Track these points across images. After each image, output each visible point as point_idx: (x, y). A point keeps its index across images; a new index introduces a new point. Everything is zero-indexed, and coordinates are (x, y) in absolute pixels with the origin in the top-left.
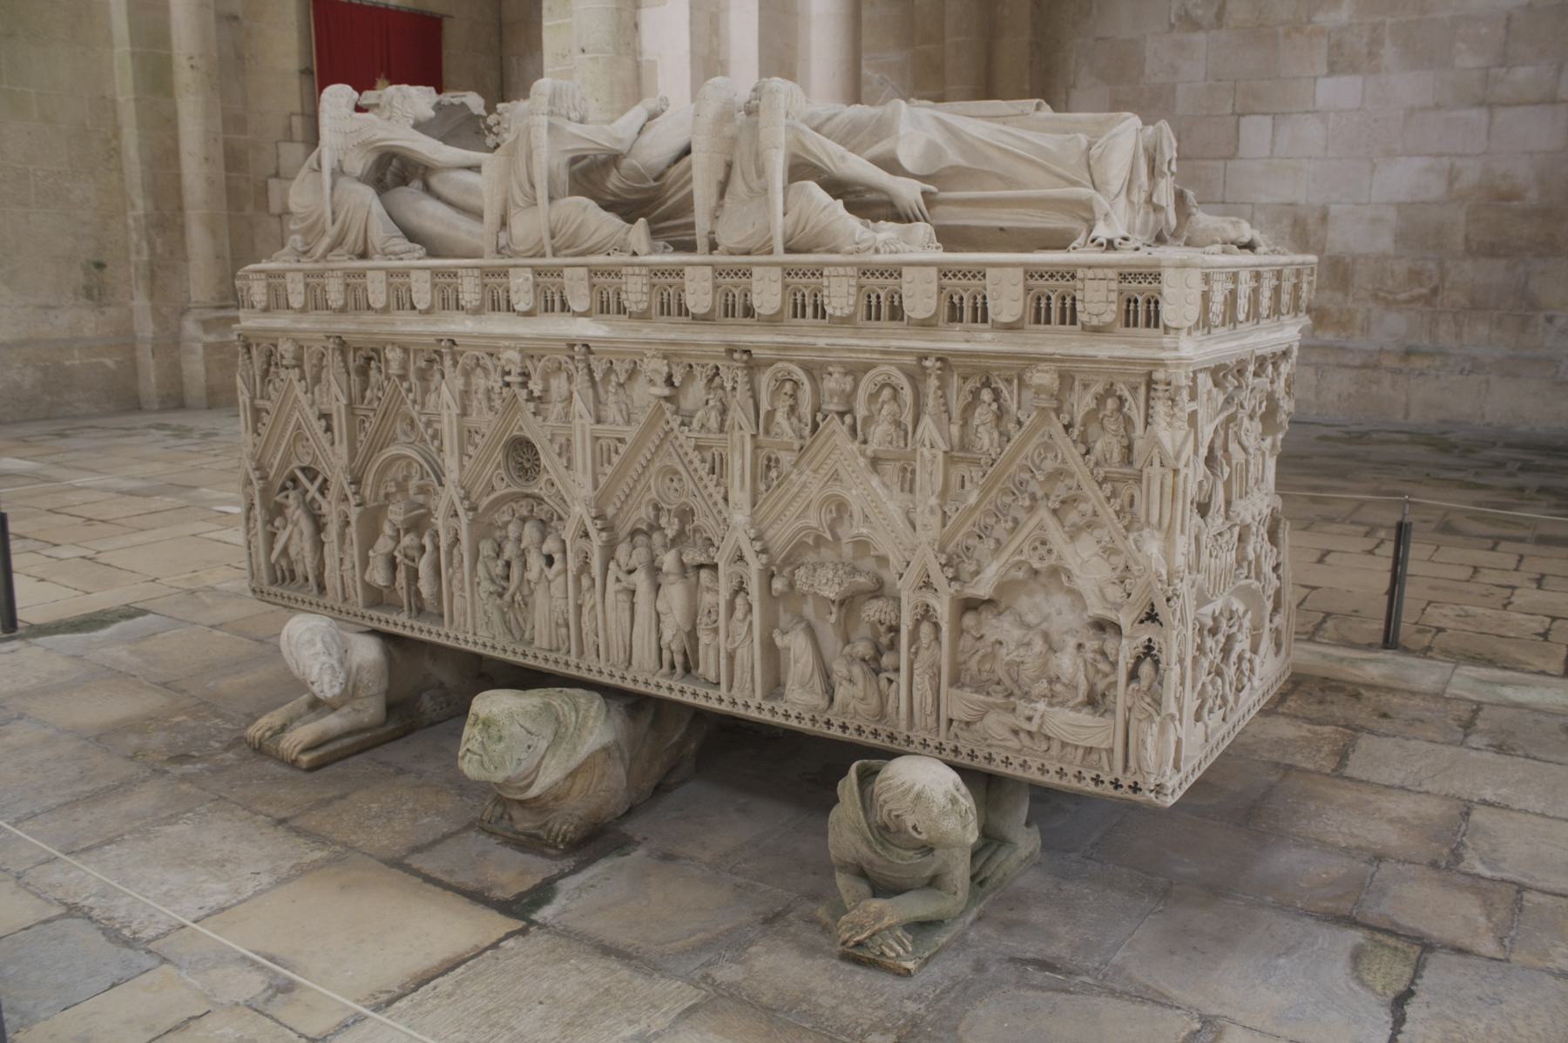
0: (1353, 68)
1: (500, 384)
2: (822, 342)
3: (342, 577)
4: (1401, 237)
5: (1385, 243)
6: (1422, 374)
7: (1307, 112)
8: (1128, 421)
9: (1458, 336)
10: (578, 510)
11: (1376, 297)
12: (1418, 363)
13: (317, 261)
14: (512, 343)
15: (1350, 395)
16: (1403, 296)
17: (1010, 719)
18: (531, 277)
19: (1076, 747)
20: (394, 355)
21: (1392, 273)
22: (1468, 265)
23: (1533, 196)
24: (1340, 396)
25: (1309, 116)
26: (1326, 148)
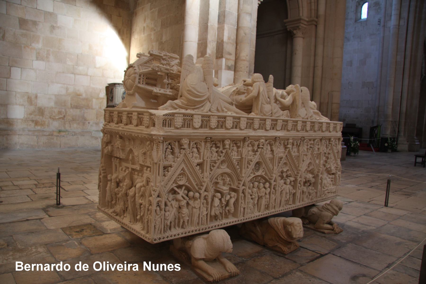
0: (43, 60)
1: (257, 148)
2: (314, 135)
3: (202, 218)
4: (56, 103)
5: (52, 104)
6: (63, 136)
7: (31, 69)
8: (336, 144)
9: (70, 127)
10: (274, 176)
11: (50, 118)
12: (62, 134)
13: (207, 112)
14: (264, 138)
15: (46, 143)
16: (57, 117)
17: (328, 191)
18: (270, 121)
19: (332, 192)
20: (227, 142)
21: (54, 112)
22: (71, 110)
23: (84, 95)
24: (43, 143)
25: (31, 70)
26: (36, 79)
